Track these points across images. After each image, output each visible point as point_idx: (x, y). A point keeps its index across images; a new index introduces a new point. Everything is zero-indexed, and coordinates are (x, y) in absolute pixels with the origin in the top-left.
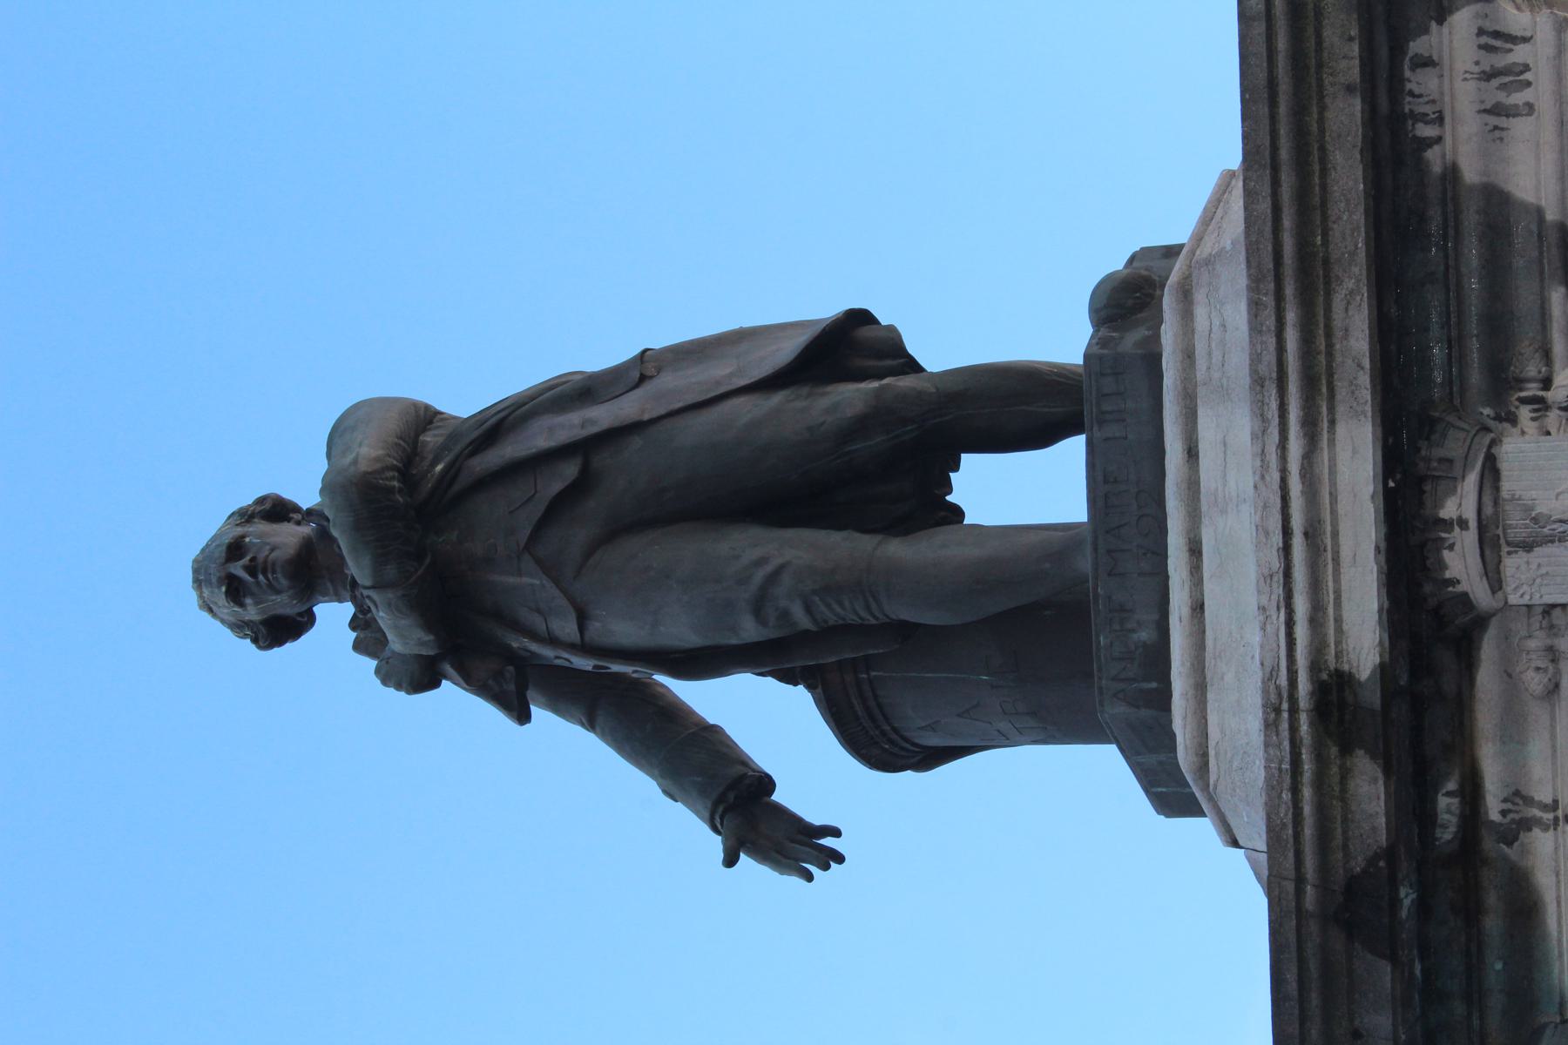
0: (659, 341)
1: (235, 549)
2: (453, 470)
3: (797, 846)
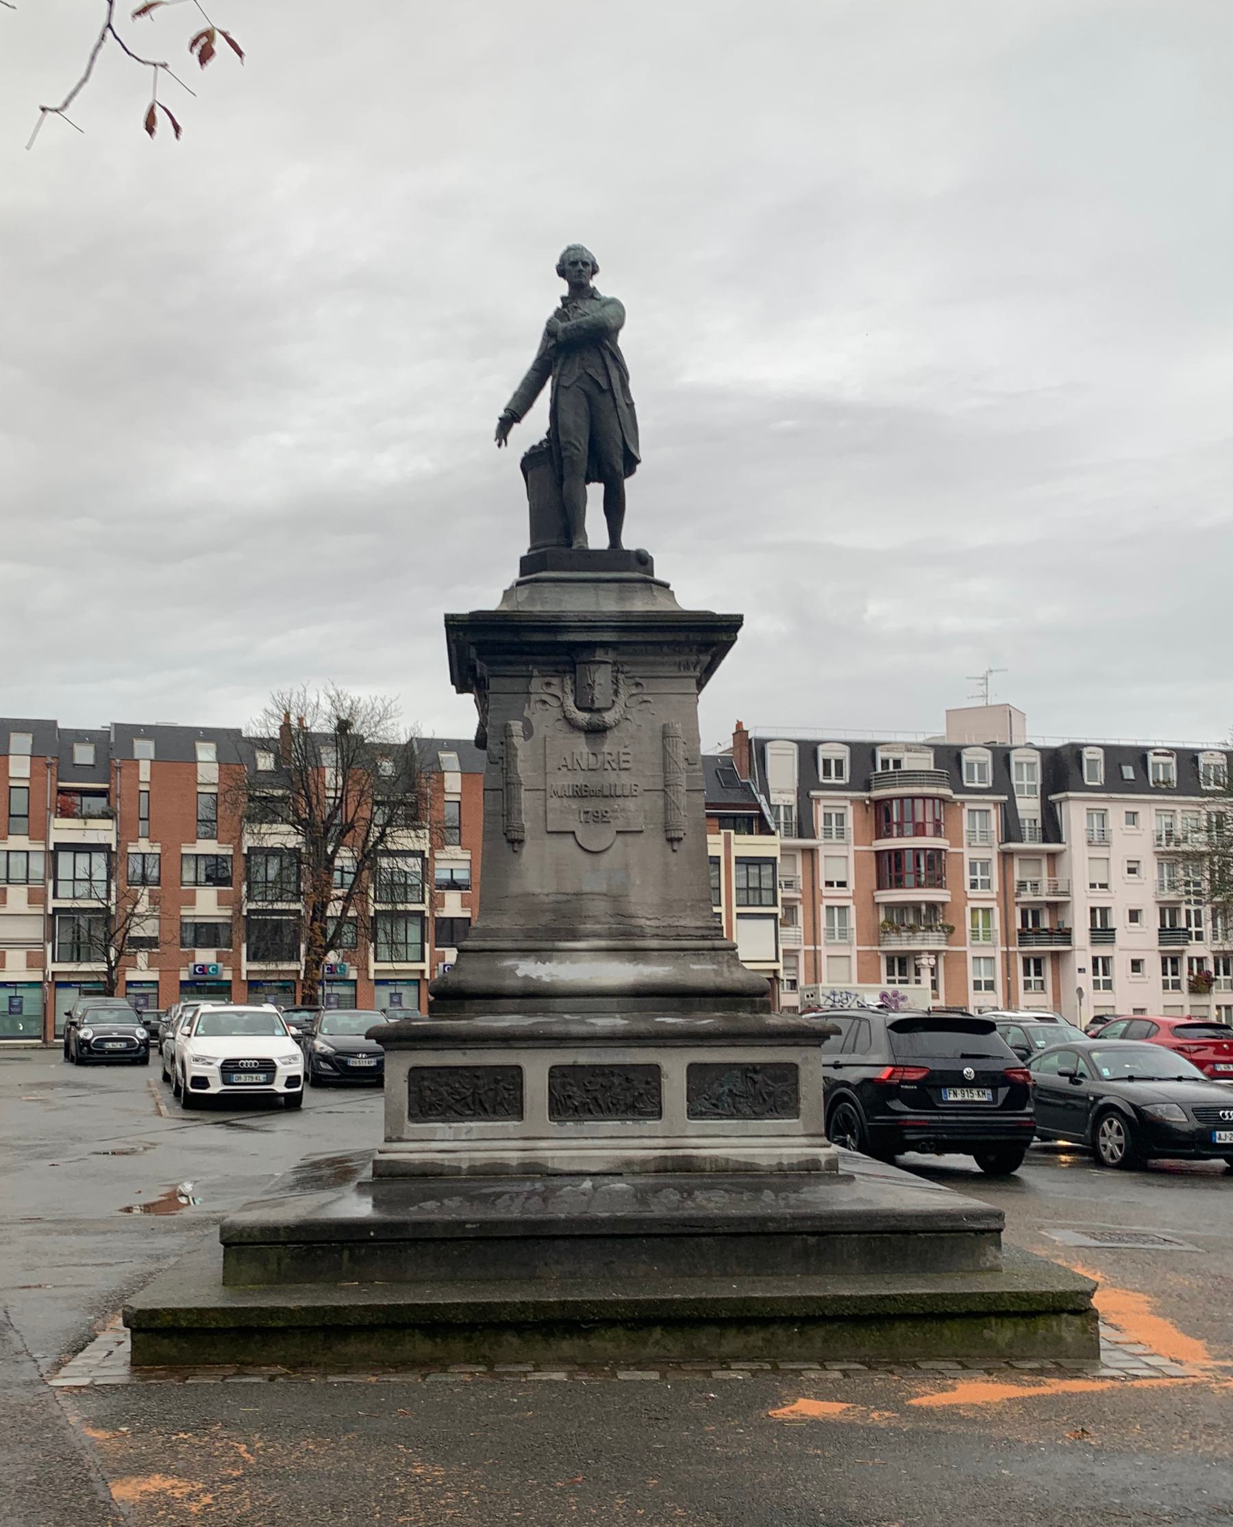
0: (636, 407)
1: (585, 264)
2: (607, 348)
3: (503, 431)
